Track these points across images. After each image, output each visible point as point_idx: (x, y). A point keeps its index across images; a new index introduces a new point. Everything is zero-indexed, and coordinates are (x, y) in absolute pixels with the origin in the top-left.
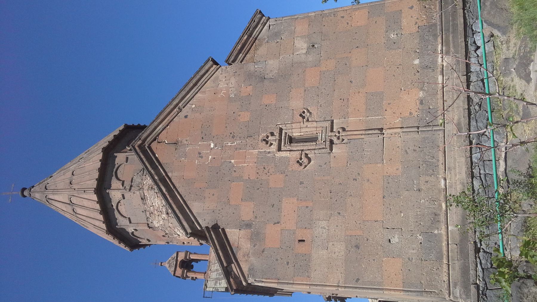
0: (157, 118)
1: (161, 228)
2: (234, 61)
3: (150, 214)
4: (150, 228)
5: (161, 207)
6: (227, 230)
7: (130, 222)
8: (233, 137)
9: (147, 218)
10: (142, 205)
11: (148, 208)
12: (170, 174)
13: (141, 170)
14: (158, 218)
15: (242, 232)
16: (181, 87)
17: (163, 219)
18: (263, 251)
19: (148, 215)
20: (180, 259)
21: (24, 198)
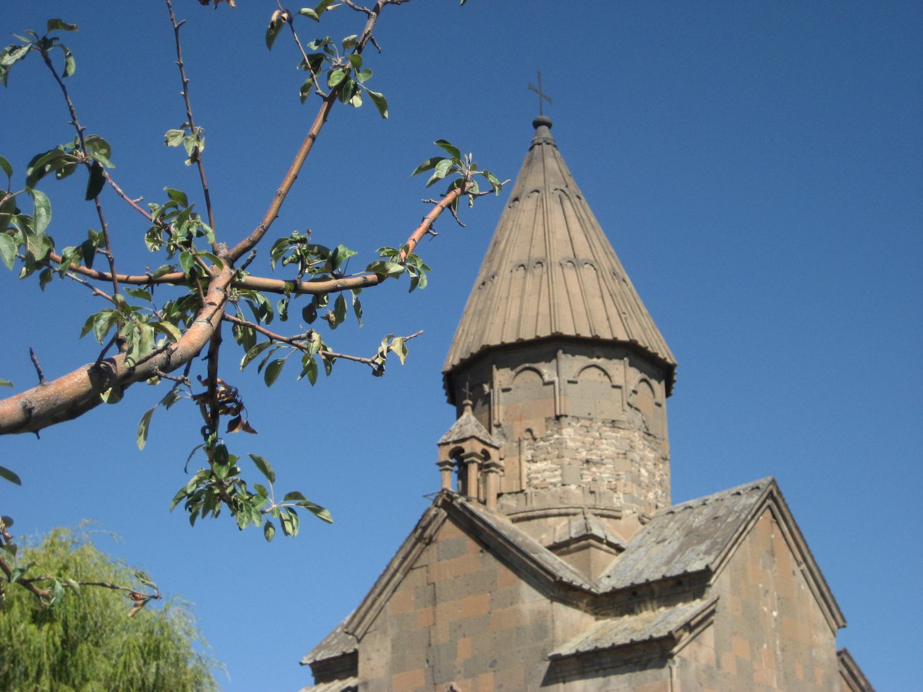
0: (797, 527)
1: (556, 436)
2: (843, 661)
3: (585, 427)
4: (558, 418)
5: (599, 452)
6: (711, 629)
7: (570, 382)
8: (783, 650)
9: (578, 419)
10: (604, 416)
11: (596, 428)
12: (748, 538)
13: (648, 430)
14: (578, 441)
15: (712, 653)
16: (823, 572)
17: (578, 449)
18: (701, 684)
20: (491, 451)
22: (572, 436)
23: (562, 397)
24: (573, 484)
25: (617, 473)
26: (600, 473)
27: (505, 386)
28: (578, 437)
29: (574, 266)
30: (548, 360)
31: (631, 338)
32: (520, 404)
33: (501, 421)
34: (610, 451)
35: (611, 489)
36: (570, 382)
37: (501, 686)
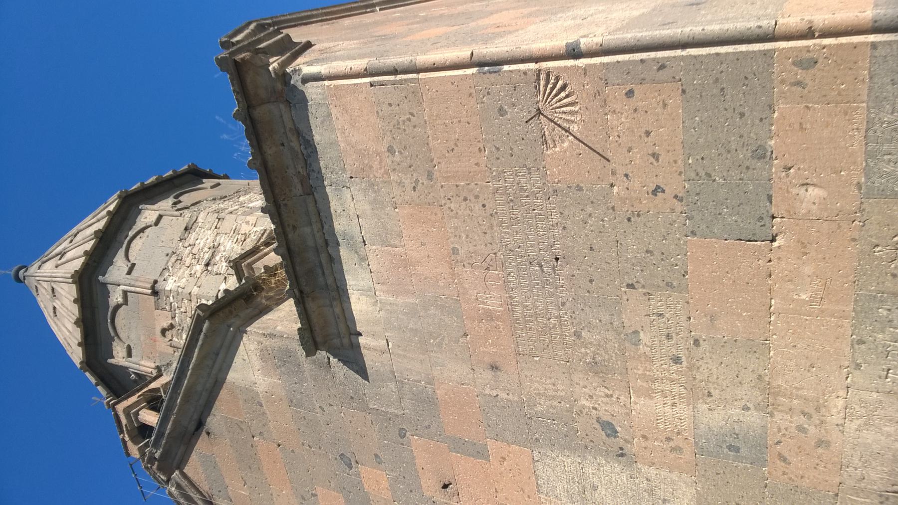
1: (171, 298)
7: (129, 273)
9: (165, 269)
19: (170, 264)
20: (153, 385)
21: (15, 282)
22: (177, 279)
23: (136, 284)
24: (219, 287)
25: (233, 231)
26: (224, 251)
27: (125, 354)
28: (182, 270)
29: (66, 253)
30: (107, 294)
31: (116, 197)
32: (142, 338)
33: (153, 365)
34: (209, 237)
35: (245, 240)
36: (129, 273)
37: (376, 456)
